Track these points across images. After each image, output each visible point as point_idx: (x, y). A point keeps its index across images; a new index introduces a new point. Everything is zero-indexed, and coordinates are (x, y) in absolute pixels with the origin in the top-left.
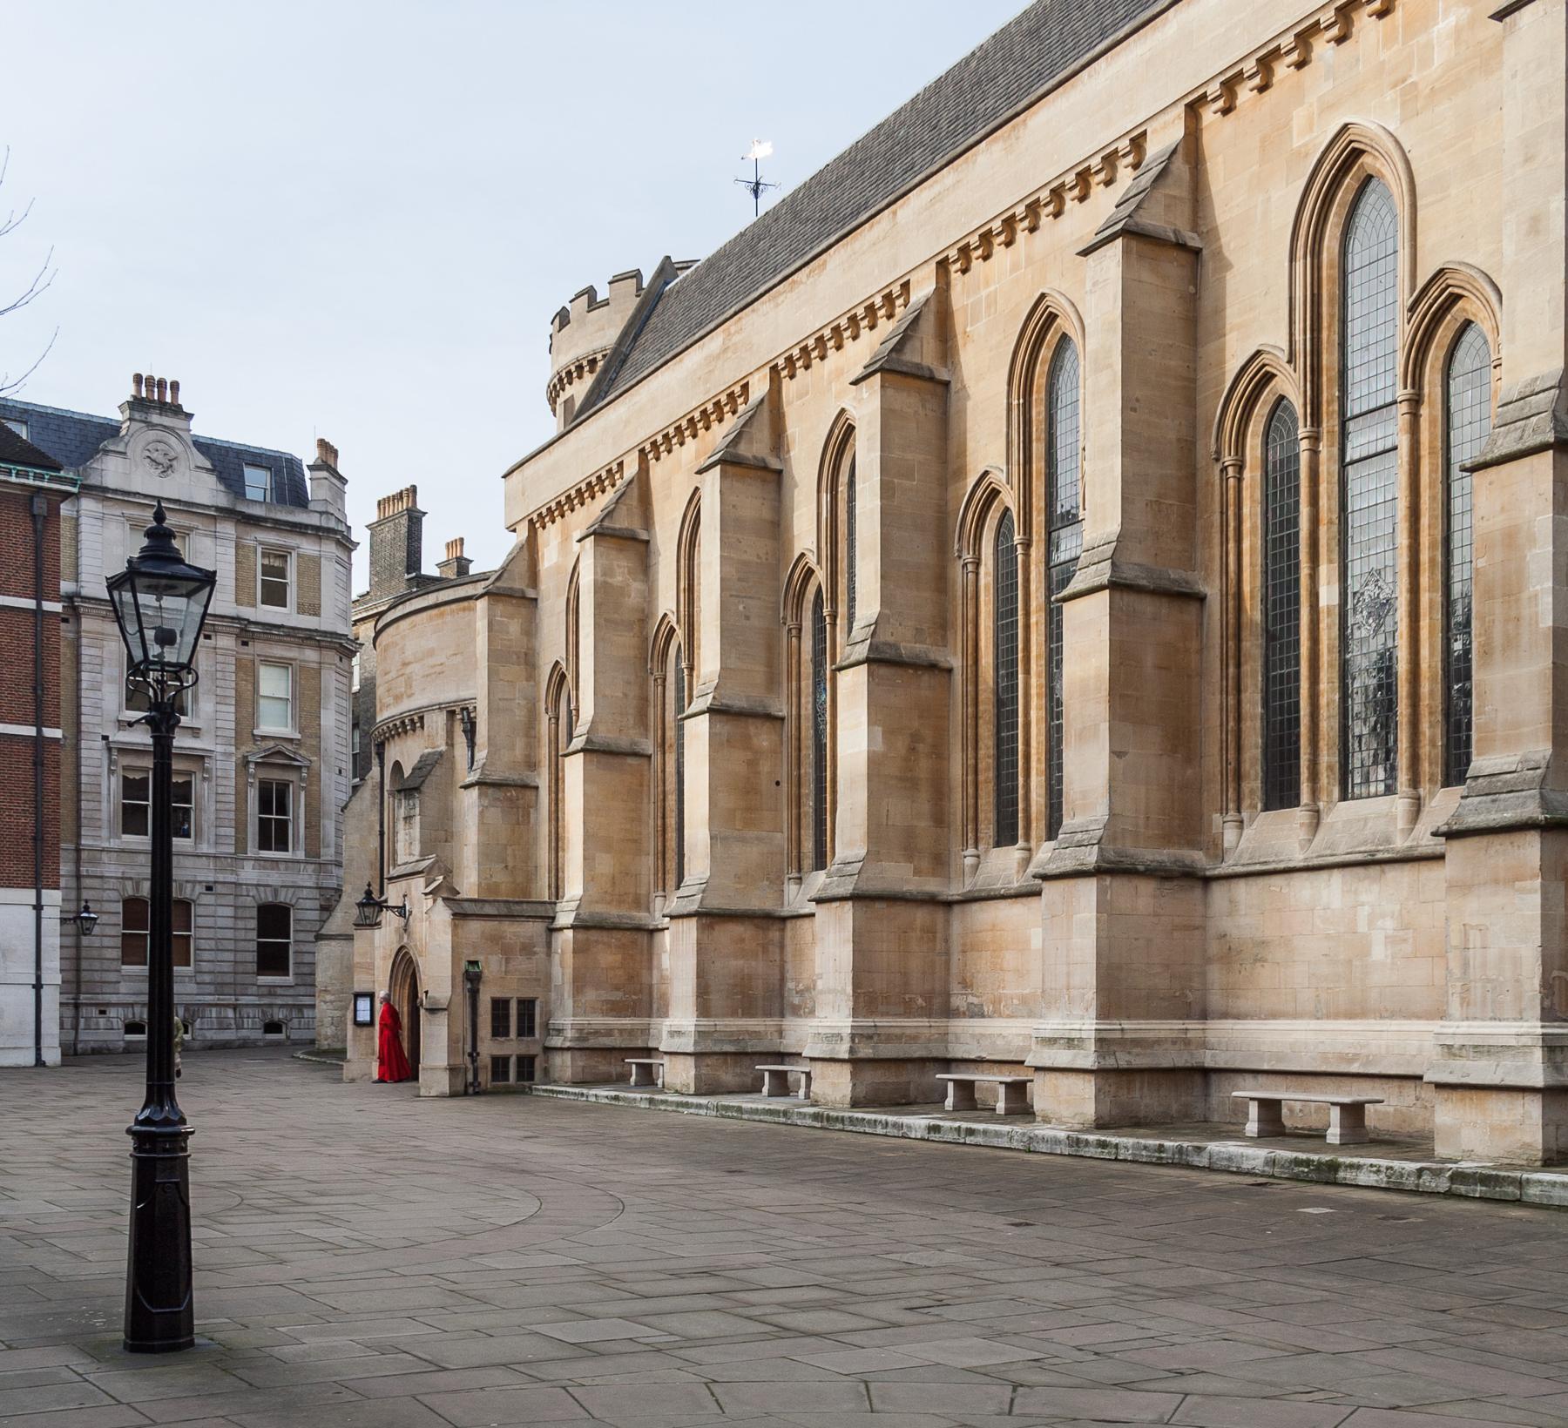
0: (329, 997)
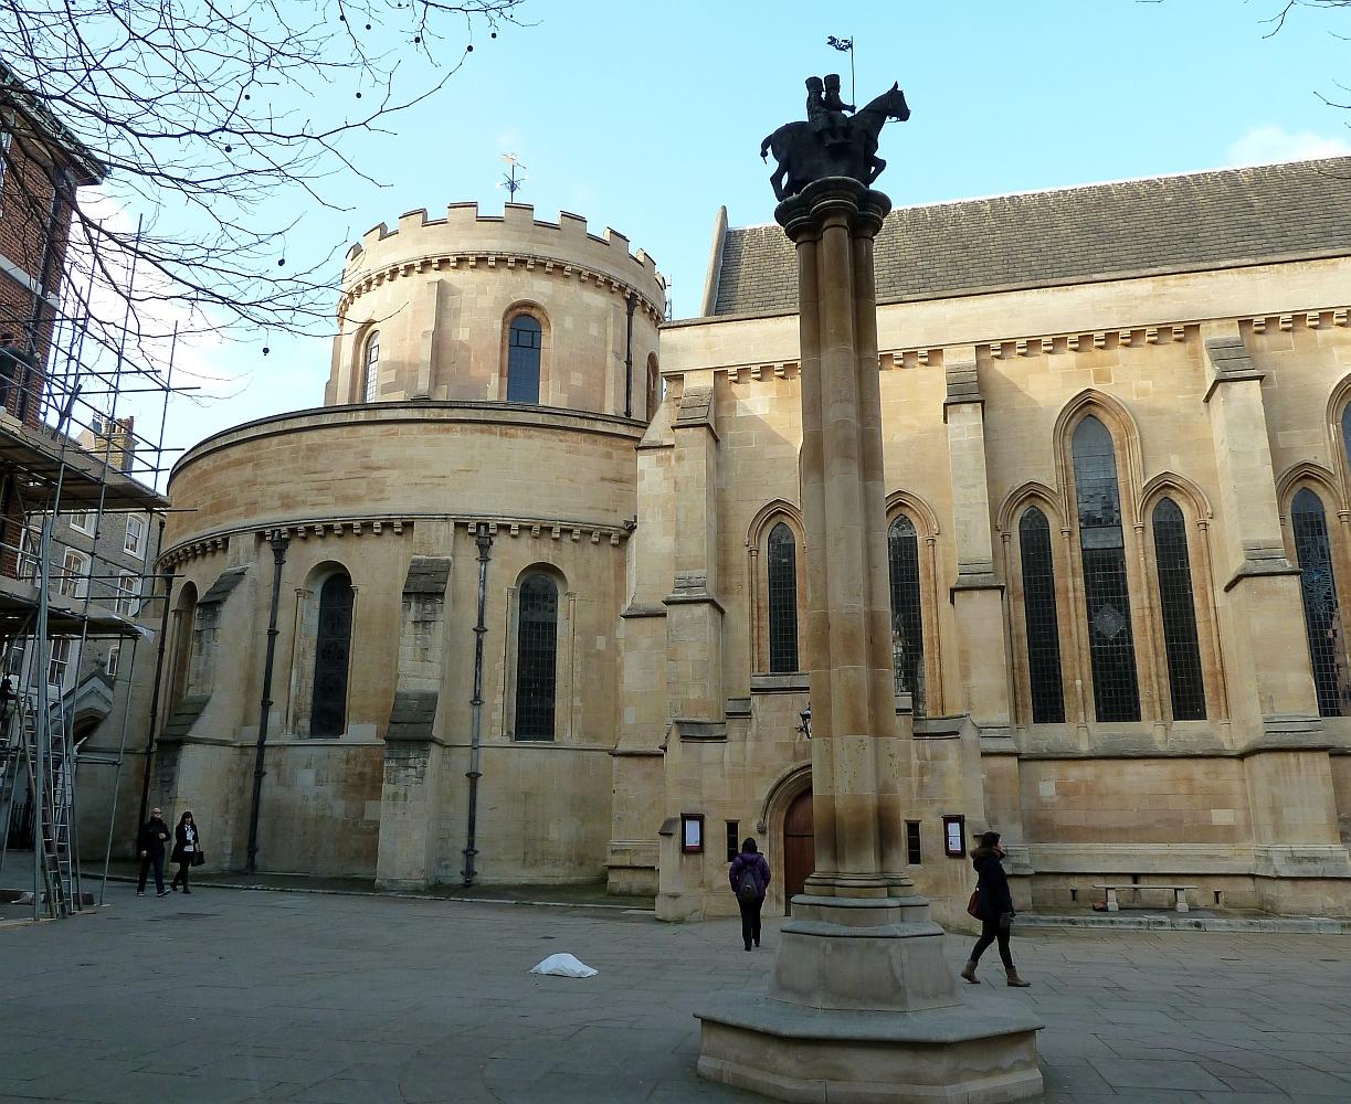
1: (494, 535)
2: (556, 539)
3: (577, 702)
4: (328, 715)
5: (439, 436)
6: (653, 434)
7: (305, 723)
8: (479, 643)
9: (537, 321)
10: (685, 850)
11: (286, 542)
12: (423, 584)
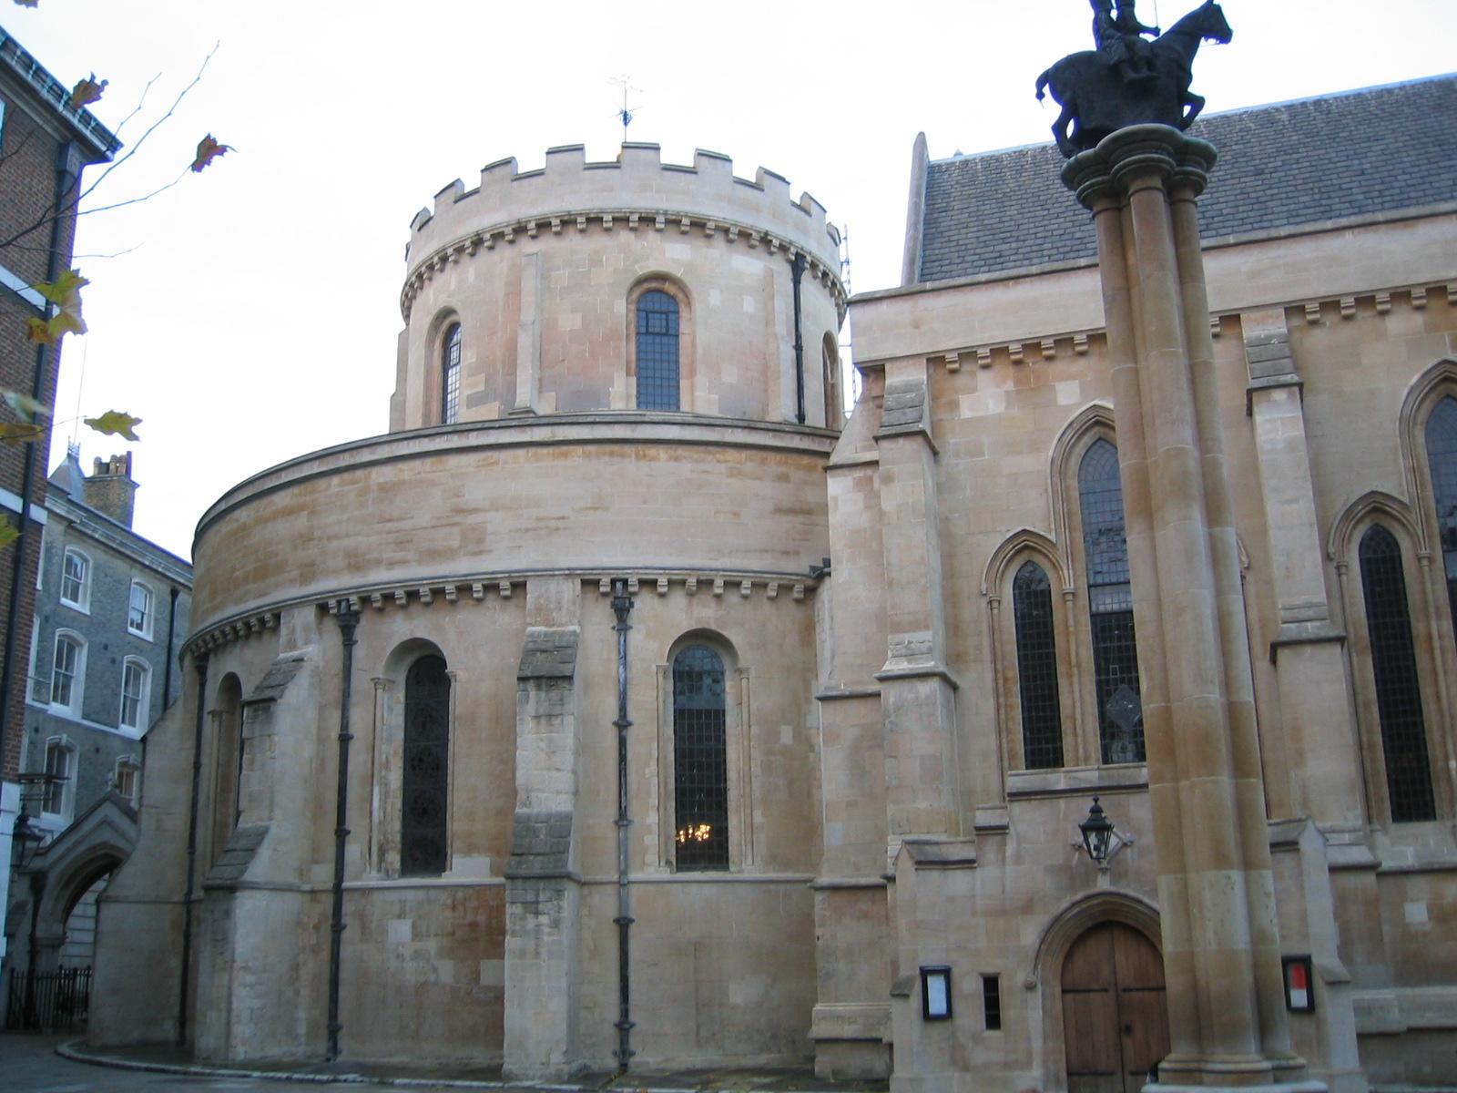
0: (249, 978)
1: (634, 594)
2: (718, 597)
3: (758, 817)
4: (424, 844)
5: (556, 463)
6: (843, 452)
7: (394, 858)
8: (622, 743)
9: (673, 298)
10: (927, 1017)
11: (356, 616)
12: (544, 665)
